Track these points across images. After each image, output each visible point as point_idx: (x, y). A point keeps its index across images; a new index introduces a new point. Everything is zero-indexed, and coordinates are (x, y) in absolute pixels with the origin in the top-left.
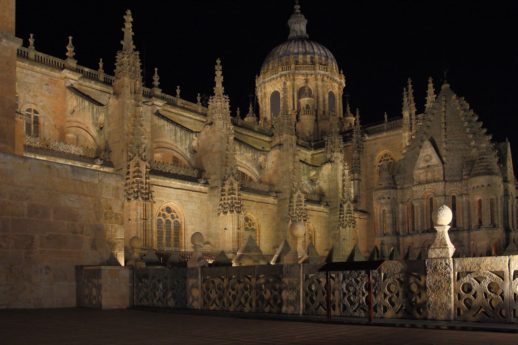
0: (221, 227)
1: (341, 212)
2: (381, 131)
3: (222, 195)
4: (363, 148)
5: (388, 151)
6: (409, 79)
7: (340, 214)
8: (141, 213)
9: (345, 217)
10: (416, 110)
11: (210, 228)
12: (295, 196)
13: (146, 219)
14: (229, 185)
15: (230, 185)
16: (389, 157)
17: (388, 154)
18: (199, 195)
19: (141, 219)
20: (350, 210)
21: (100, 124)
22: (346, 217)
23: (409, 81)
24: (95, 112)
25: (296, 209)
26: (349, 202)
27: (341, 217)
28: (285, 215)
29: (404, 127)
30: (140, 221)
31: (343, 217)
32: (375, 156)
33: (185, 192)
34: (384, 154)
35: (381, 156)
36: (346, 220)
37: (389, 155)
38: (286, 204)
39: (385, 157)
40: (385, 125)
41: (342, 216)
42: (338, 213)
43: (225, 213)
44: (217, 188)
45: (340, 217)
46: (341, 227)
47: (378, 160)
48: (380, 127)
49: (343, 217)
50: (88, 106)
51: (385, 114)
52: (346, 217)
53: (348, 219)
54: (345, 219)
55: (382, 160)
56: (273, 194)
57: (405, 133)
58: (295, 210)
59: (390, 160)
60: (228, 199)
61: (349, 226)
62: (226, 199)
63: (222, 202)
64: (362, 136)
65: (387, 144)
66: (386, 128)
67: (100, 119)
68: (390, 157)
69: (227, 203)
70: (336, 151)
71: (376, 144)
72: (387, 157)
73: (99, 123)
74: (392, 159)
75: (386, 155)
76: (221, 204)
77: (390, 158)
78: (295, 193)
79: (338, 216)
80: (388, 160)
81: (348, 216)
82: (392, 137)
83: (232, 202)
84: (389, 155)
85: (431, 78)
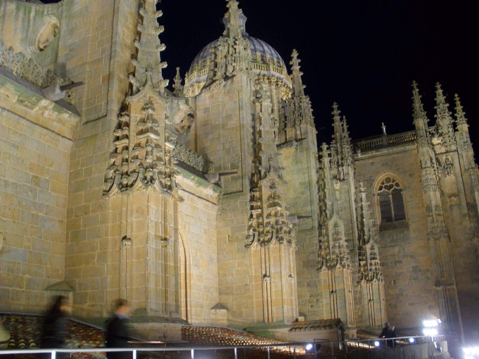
0: (253, 272)
1: (361, 258)
2: (378, 147)
3: (252, 208)
5: (392, 173)
6: (414, 82)
7: (360, 260)
8: (156, 223)
9: (369, 265)
10: (428, 120)
11: (226, 275)
13: (165, 239)
14: (268, 188)
15: (271, 187)
16: (393, 182)
17: (391, 178)
18: (207, 206)
19: (156, 236)
20: (374, 254)
21: (39, 42)
22: (371, 264)
23: (414, 84)
24: (32, 18)
25: (334, 247)
26: (371, 241)
27: (362, 265)
28: (312, 257)
29: (420, 139)
30: (154, 241)
31: (366, 265)
32: (373, 181)
34: (386, 177)
36: (371, 269)
37: (393, 179)
38: (315, 237)
39: (387, 182)
40: (385, 140)
41: (362, 263)
42: (357, 259)
43: (264, 243)
44: (242, 195)
45: (360, 265)
46: (363, 281)
47: (378, 186)
48: (370, 143)
49: (366, 265)
50: (15, 11)
51: (382, 125)
53: (373, 268)
54: (369, 268)
55: (383, 186)
56: (294, 219)
57: (422, 147)
58: (332, 248)
59: (395, 187)
60: (269, 215)
61: (377, 278)
62: (265, 215)
63: (254, 222)
64: (353, 152)
66: (385, 143)
67: (41, 32)
68: (395, 183)
69: (269, 223)
70: (345, 164)
71: (372, 164)
72: (389, 182)
73: (37, 39)
74: (397, 185)
75: (388, 180)
76: (250, 226)
77: (394, 184)
78: (331, 217)
79: (357, 264)
80: (391, 186)
81: (373, 263)
82: (395, 155)
83: (277, 223)
84: (393, 179)
85: (439, 83)
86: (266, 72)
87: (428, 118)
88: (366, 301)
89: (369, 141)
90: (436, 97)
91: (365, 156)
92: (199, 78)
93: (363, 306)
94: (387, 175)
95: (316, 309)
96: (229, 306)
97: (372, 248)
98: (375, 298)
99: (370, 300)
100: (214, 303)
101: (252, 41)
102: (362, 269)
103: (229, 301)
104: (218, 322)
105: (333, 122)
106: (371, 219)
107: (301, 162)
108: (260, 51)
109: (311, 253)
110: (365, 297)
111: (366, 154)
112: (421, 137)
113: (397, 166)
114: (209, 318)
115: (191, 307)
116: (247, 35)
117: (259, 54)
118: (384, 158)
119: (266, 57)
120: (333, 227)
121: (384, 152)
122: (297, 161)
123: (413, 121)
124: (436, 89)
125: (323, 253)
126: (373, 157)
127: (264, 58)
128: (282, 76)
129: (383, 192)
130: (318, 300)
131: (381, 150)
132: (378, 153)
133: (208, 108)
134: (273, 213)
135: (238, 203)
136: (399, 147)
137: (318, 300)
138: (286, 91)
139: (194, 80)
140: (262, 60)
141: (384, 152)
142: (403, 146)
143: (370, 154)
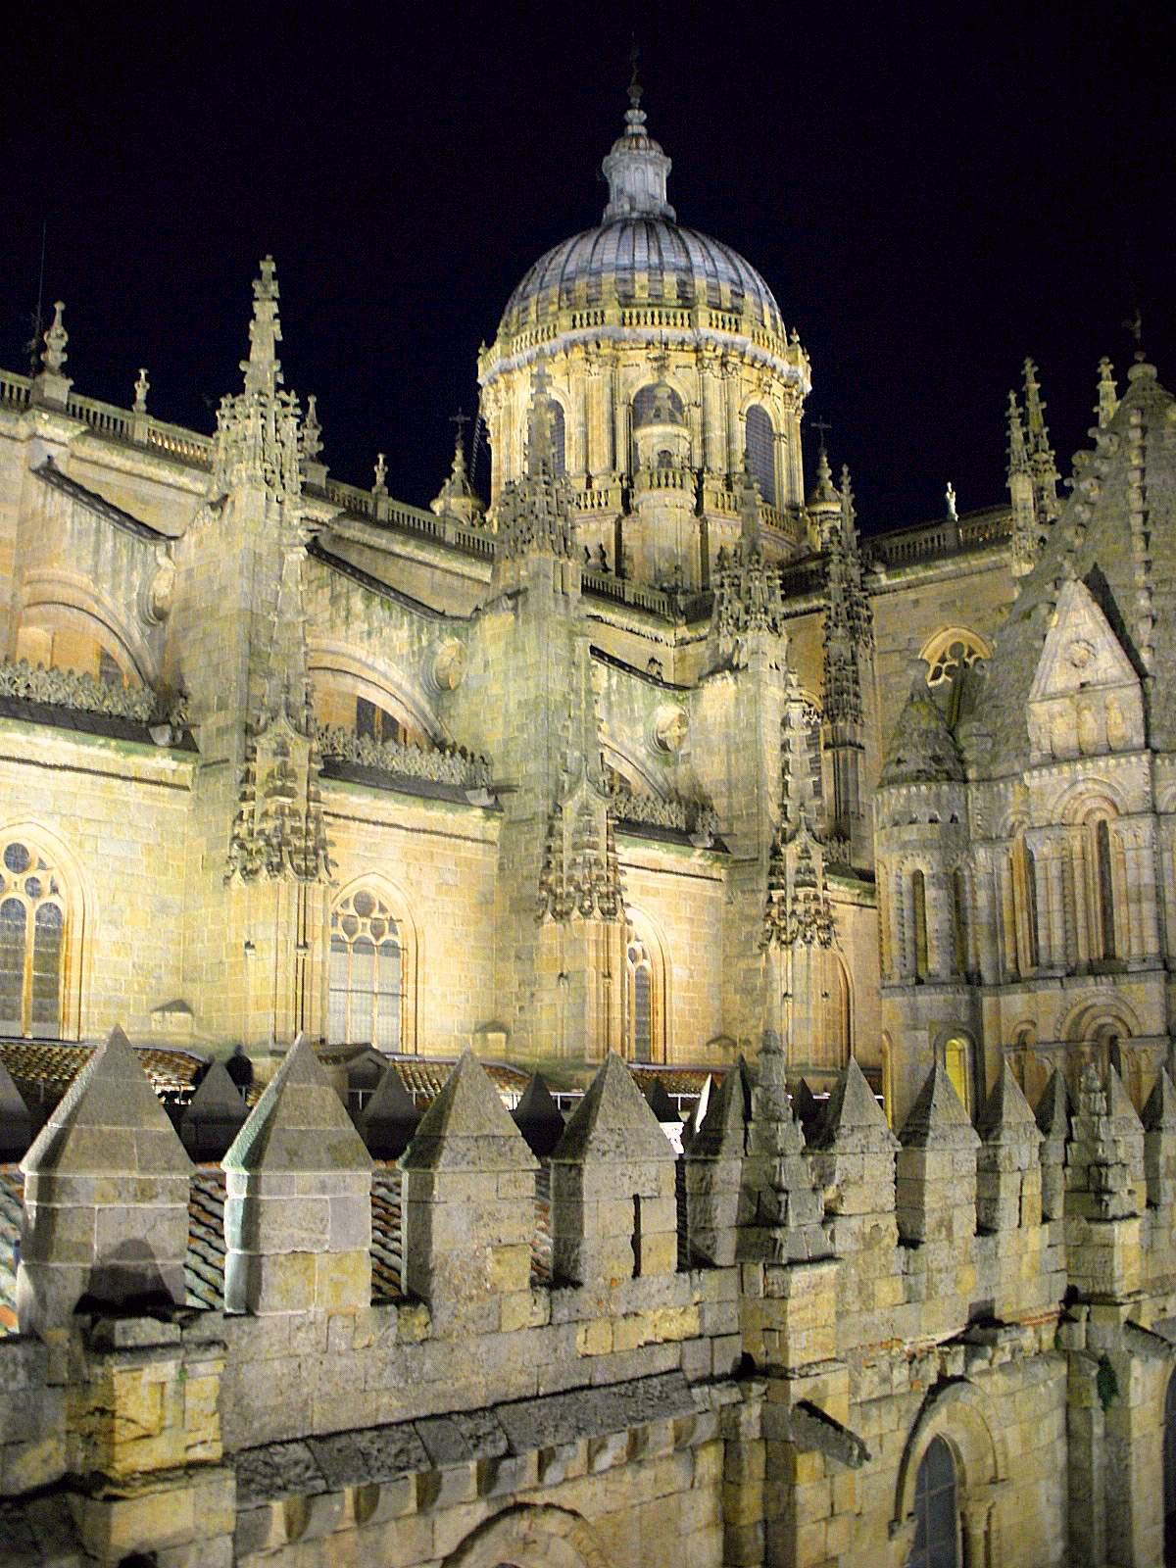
1: (774, 880)
3: (244, 798)
4: (869, 619)
5: (964, 631)
6: (1028, 362)
7: (771, 887)
12: (570, 807)
15: (275, 754)
16: (970, 655)
17: (965, 644)
20: (812, 871)
22: (795, 899)
23: (1028, 368)
25: (574, 864)
26: (803, 837)
27: (775, 899)
29: (1015, 538)
31: (783, 899)
33: (93, 783)
34: (950, 643)
35: (939, 654)
36: (794, 912)
38: (536, 839)
41: (776, 894)
42: (764, 883)
44: (227, 768)
46: (773, 943)
49: (783, 899)
52: (795, 899)
53: (800, 908)
54: (789, 909)
55: (944, 666)
58: (570, 868)
60: (265, 814)
62: (257, 815)
64: (863, 571)
65: (958, 604)
66: (950, 543)
68: (974, 657)
70: (752, 624)
71: (916, 602)
75: (956, 649)
78: (571, 791)
79: (763, 897)
81: (801, 897)
82: (976, 579)
86: (687, 334)
87: (1058, 471)
88: (778, 998)
89: (910, 538)
90: (1097, 403)
91: (898, 580)
92: (506, 360)
93: (770, 1010)
94: (954, 635)
95: (527, 1016)
96: (194, 1006)
97: (806, 854)
98: (798, 990)
99: (786, 995)
100: (165, 998)
101: (677, 232)
102: (774, 912)
103: (196, 994)
104: (168, 1039)
105: (1009, 428)
106: (808, 775)
107: (524, 650)
108: (677, 269)
109: (526, 878)
110: (775, 985)
111: (899, 575)
112: (1019, 529)
113: (977, 610)
114: (146, 1029)
115: (88, 1007)
116: (672, 213)
117: (670, 279)
118: (946, 586)
119: (693, 286)
120: (574, 815)
121: (946, 569)
122: (516, 648)
123: (1006, 480)
124: (1099, 378)
125: (551, 879)
126: (923, 582)
127: (688, 289)
128: (738, 338)
129: (942, 685)
130: (533, 995)
131: (938, 563)
132: (931, 573)
133: (192, 570)
134: (272, 809)
135: (220, 787)
136: (984, 554)
137: (533, 995)
138: (760, 380)
139: (496, 367)
140: (682, 295)
141: (946, 569)
142: (993, 552)
143: (910, 575)
